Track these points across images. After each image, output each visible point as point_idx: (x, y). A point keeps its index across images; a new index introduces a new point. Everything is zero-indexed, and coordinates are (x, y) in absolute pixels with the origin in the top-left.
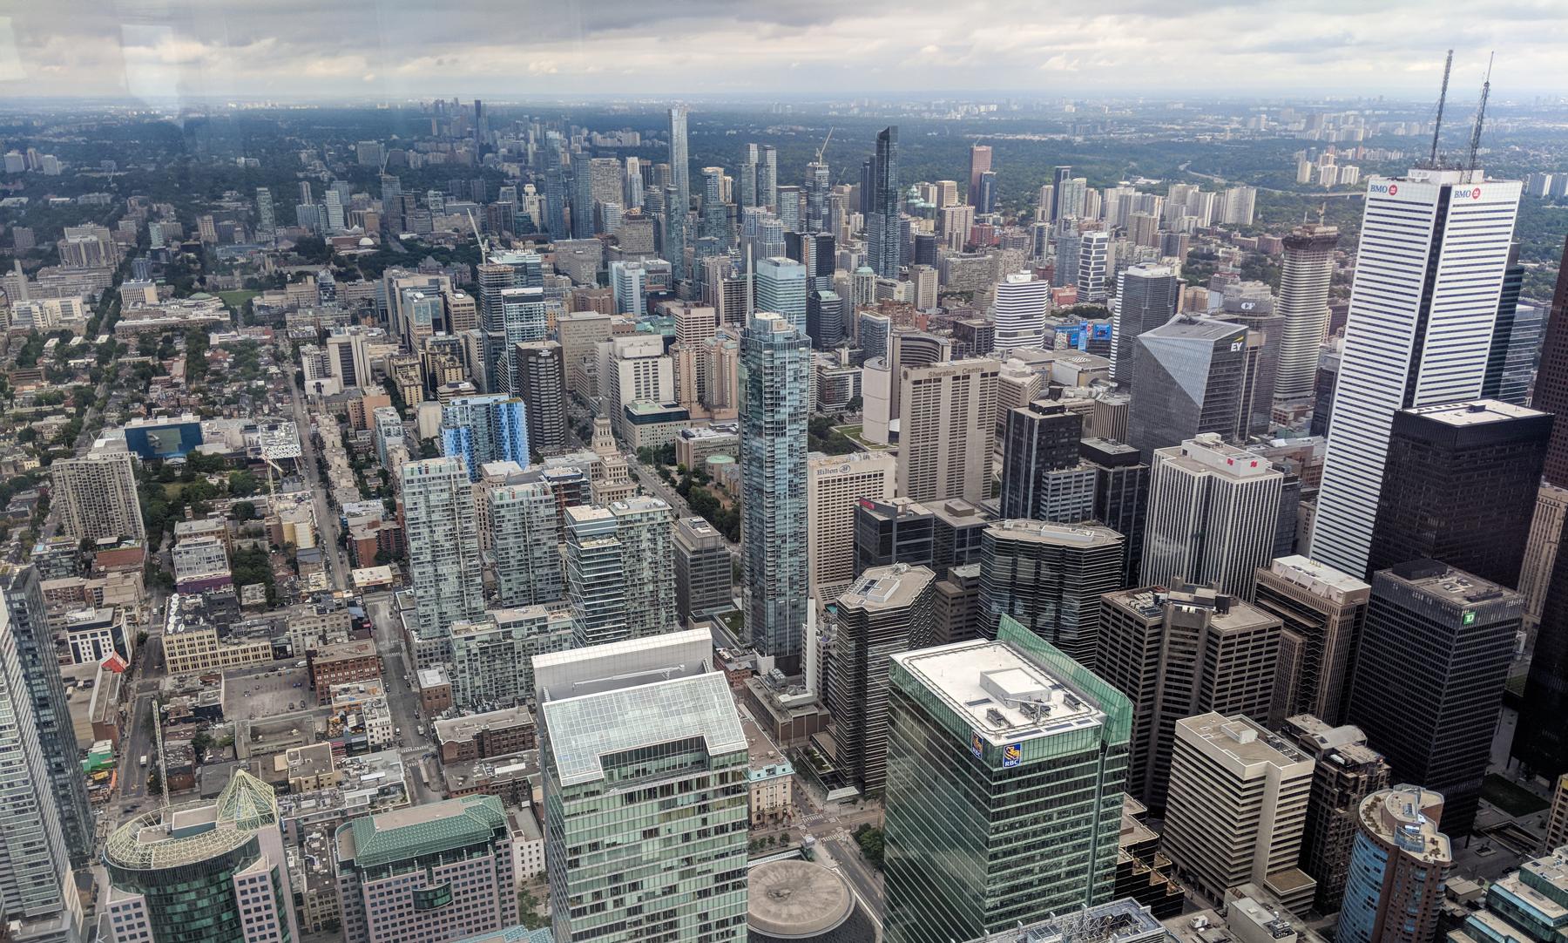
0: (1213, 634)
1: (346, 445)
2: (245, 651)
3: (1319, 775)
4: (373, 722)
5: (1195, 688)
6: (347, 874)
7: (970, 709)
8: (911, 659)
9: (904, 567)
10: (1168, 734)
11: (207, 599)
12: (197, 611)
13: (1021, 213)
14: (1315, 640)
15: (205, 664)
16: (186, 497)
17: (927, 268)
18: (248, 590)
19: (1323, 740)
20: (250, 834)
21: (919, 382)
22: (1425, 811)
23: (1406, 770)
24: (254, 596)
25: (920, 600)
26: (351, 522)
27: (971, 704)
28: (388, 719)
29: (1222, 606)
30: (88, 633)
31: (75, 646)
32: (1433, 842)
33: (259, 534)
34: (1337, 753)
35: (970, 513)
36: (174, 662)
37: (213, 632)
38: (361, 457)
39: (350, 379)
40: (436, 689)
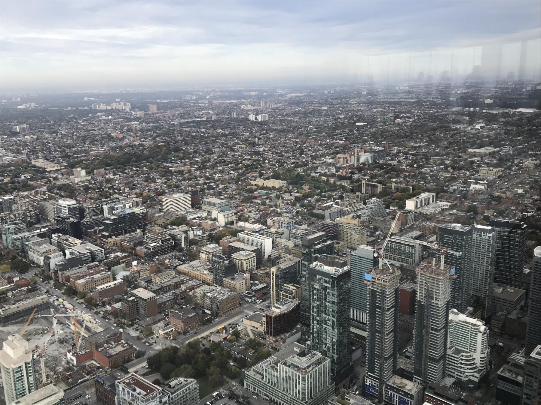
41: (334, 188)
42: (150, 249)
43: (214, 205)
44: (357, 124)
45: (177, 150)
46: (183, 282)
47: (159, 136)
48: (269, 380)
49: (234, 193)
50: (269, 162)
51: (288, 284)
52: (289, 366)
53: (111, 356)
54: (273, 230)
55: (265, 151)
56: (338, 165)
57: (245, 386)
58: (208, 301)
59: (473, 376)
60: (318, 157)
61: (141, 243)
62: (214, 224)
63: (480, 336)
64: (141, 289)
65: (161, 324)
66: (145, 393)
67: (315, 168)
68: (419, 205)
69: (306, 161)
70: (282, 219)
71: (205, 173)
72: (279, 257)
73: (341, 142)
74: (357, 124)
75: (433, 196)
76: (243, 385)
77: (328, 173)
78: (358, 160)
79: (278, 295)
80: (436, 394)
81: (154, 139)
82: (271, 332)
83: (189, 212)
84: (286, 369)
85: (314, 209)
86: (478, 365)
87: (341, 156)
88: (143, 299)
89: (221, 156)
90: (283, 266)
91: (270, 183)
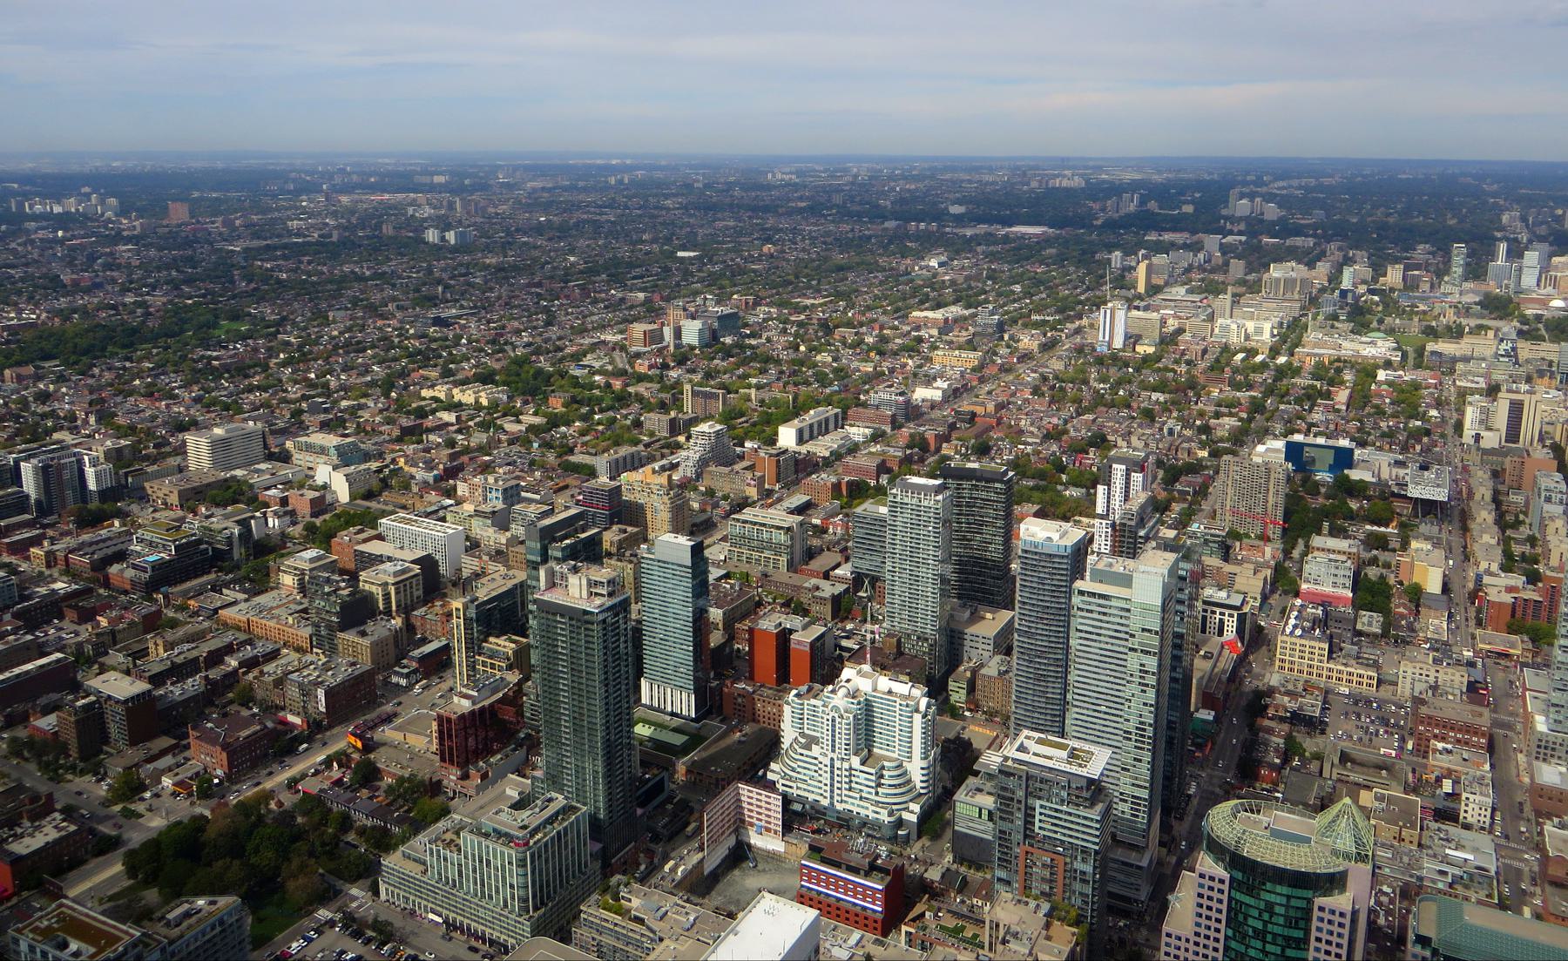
1: (1496, 500)
2: (1350, 674)
4: (1472, 797)
6: (1418, 949)
11: (1326, 612)
12: (1316, 622)
15: (1310, 674)
16: (1325, 513)
18: (1365, 616)
20: (1339, 865)
24: (1370, 624)
26: (1486, 580)
28: (1490, 801)
30: (1218, 610)
31: (1204, 618)
33: (1387, 566)
36: (1282, 661)
37: (1326, 646)
38: (1510, 518)
39: (1513, 432)
40: (1552, 788)
41: (622, 399)
42: (144, 570)
43: (323, 451)
44: (680, 254)
45: (236, 317)
46: (229, 649)
47: (189, 281)
48: (440, 874)
49: (378, 419)
50: (470, 342)
51: (498, 637)
52: (487, 835)
53: (17, 860)
54: (469, 508)
55: (460, 317)
56: (634, 349)
57: (383, 896)
58: (293, 692)
59: (906, 809)
60: (586, 330)
61: (121, 556)
62: (323, 497)
63: (917, 718)
64: (112, 675)
65: (168, 760)
66: (92, 950)
67: (577, 357)
68: (806, 435)
69: (560, 338)
70: (491, 479)
71: (308, 370)
72: (477, 576)
73: (641, 296)
74: (680, 254)
75: (836, 415)
76: (376, 893)
77: (610, 368)
78: (678, 333)
79: (472, 667)
80: (825, 861)
81: (177, 288)
82: (451, 754)
83: (257, 471)
84: (480, 844)
85: (571, 451)
86: (919, 785)
87: (639, 329)
88: (118, 702)
89: (349, 329)
90: (483, 592)
91: (466, 396)
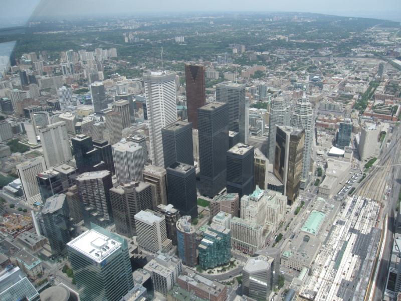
0: (137, 193)
3: (166, 217)
5: (136, 205)
7: (91, 254)
8: (72, 243)
9: (57, 195)
10: (133, 218)
13: (57, 60)
14: (158, 184)
17: (34, 84)
19: (165, 210)
21: (43, 132)
22: (189, 221)
23: (182, 214)
25: (63, 205)
27: (91, 252)
29: (137, 185)
32: (191, 228)
34: (168, 212)
35: (69, 168)
